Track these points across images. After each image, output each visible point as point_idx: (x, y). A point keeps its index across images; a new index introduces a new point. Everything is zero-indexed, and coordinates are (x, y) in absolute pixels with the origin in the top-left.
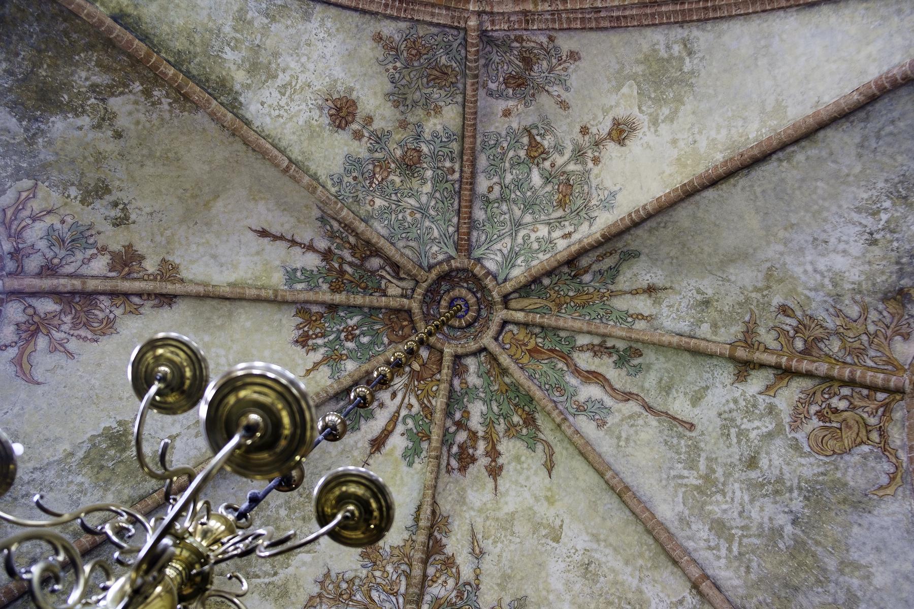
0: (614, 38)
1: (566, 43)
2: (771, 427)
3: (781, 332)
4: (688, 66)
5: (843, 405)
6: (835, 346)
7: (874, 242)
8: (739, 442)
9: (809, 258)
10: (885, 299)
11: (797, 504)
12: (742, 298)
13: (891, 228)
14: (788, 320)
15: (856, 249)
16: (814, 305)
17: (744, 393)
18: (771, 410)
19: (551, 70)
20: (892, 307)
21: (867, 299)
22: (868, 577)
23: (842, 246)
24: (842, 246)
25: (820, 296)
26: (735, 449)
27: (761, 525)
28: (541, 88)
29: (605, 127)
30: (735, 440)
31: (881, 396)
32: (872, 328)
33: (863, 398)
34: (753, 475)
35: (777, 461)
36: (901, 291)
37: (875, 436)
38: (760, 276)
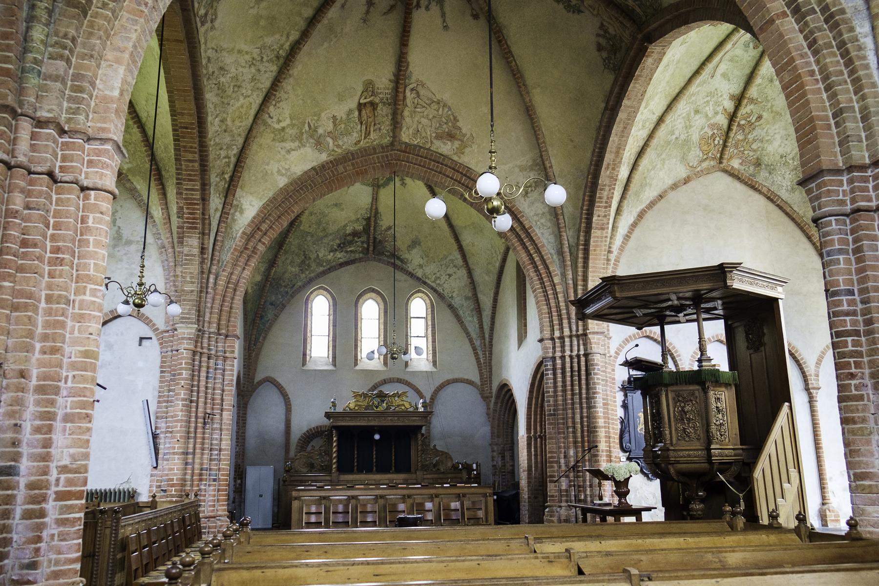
2: (710, 115)
3: (749, 115)
5: (716, 142)
6: (740, 137)
7: (782, 157)
8: (705, 103)
9: (781, 132)
10: (758, 159)
11: (683, 137)
12: (769, 98)
13: (786, 164)
14: (754, 119)
15: (781, 151)
16: (760, 131)
17: (725, 99)
18: (716, 113)
20: (754, 161)
21: (759, 153)
22: (661, 169)
23: (783, 145)
24: (783, 145)
25: (763, 133)
26: (702, 102)
27: (675, 125)
30: (705, 100)
31: (718, 155)
32: (746, 152)
33: (718, 149)
34: (692, 114)
35: (697, 123)
36: (760, 164)
37: (705, 157)
38: (778, 109)
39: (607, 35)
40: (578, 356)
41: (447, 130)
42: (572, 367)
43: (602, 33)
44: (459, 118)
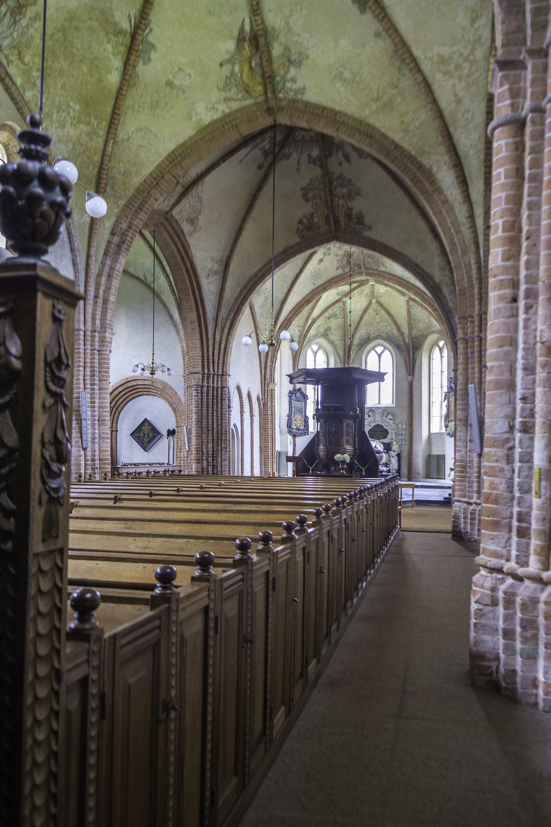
0: (329, 277)
1: (340, 271)
4: (312, 281)
19: (342, 262)
28: (344, 255)
29: (324, 260)
39: (311, 220)
40: (217, 388)
41: (192, 217)
42: (213, 394)
43: (309, 217)
44: (202, 213)
